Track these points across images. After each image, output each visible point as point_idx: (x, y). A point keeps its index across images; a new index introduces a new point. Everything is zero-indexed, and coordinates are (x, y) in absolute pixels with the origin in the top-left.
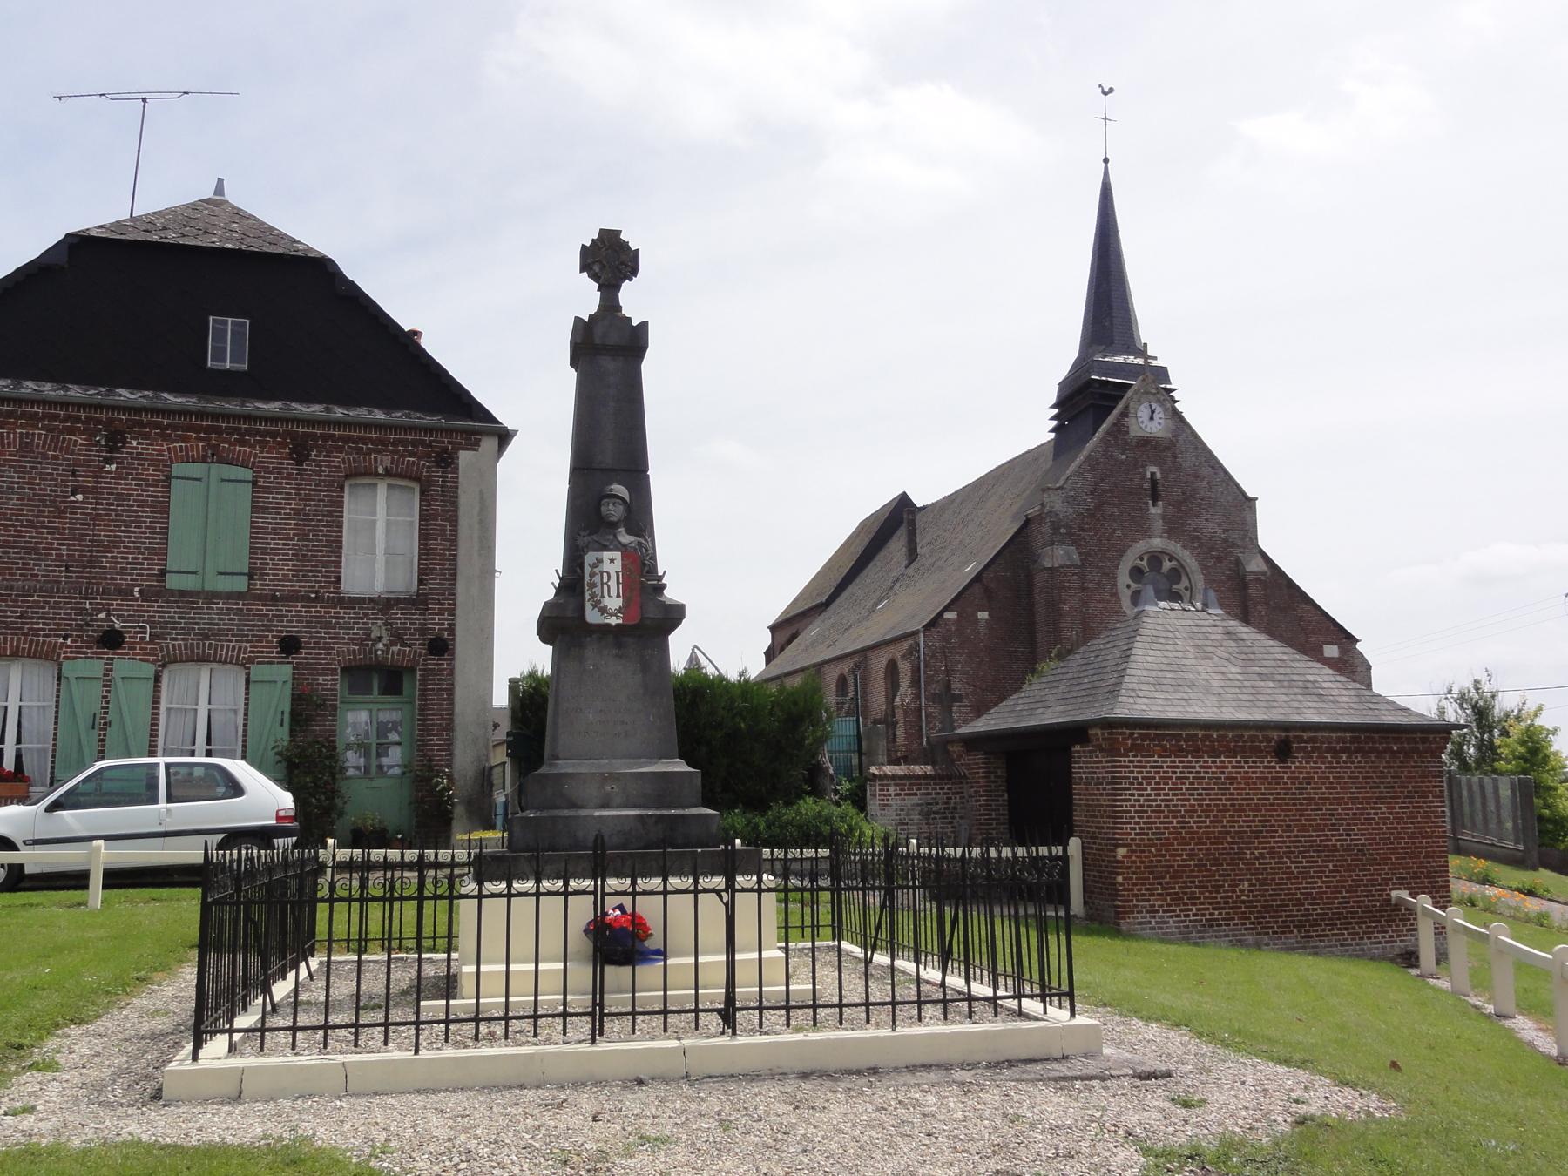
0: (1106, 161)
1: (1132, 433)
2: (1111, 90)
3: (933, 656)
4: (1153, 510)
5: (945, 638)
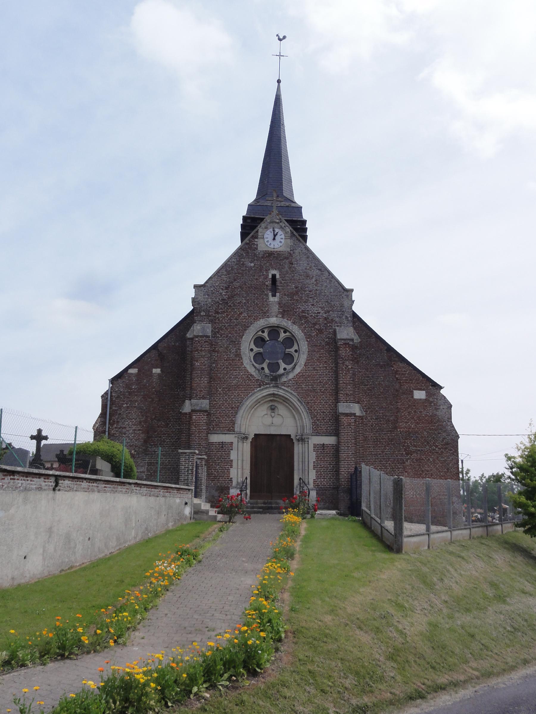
0: (279, 81)
1: (259, 249)
2: (284, 37)
3: (118, 397)
4: (271, 299)
5: (128, 386)
